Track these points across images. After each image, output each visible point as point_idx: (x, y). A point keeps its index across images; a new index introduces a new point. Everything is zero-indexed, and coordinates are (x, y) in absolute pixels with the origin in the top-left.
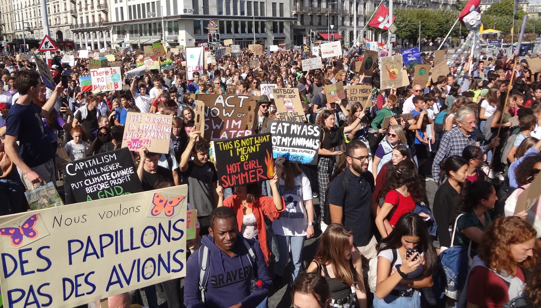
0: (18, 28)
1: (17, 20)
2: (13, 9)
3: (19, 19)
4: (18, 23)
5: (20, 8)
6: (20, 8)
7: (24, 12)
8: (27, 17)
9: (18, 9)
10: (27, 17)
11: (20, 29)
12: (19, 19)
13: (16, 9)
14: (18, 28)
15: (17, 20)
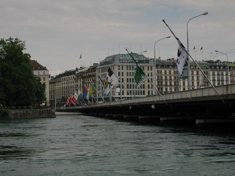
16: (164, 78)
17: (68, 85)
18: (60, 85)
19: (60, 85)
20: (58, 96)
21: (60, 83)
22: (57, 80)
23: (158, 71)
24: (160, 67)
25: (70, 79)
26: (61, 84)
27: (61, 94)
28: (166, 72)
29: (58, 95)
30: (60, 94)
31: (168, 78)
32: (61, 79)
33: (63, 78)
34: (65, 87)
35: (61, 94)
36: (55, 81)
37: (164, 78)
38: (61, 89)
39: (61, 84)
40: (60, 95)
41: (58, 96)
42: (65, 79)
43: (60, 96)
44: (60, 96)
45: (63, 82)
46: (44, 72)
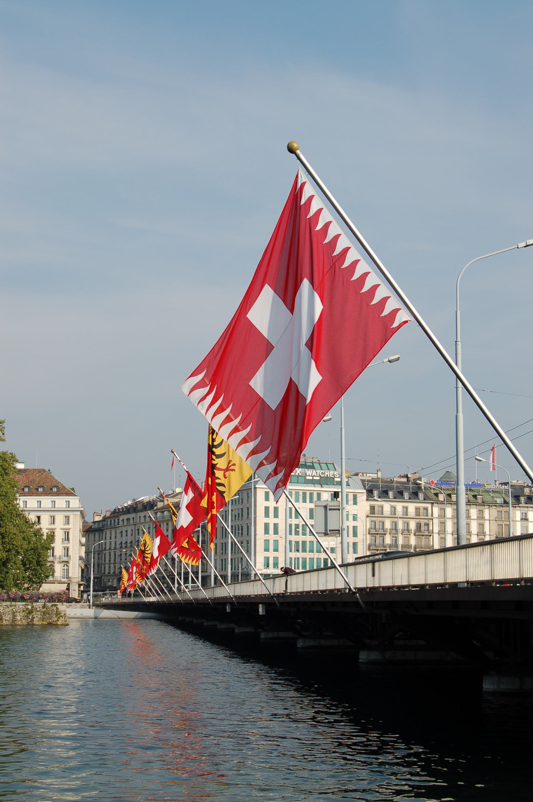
0: (107, 572)
1: (107, 561)
2: (104, 548)
3: (110, 560)
4: (107, 566)
5: (113, 548)
6: (113, 548)
7: (118, 553)
8: (121, 560)
9: (110, 549)
10: (121, 560)
11: (109, 573)
12: (110, 560)
13: (107, 548)
14: (107, 572)
15: (107, 561)
16: (388, 525)
17: (135, 538)
18: (116, 537)
19: (116, 537)
20: (110, 567)
21: (116, 532)
22: (113, 522)
23: (372, 508)
24: (395, 498)
25: (142, 520)
26: (118, 535)
27: (118, 560)
28: (394, 509)
29: (110, 563)
30: (115, 560)
31: (400, 526)
32: (118, 520)
33: (125, 517)
34: (129, 542)
35: (118, 560)
36: (103, 525)
37: (388, 525)
38: (118, 546)
39: (118, 535)
40: (115, 563)
41: (110, 567)
42: (128, 520)
43: (115, 567)
44: (115, 567)
45: (124, 530)
46: (404, 507)
